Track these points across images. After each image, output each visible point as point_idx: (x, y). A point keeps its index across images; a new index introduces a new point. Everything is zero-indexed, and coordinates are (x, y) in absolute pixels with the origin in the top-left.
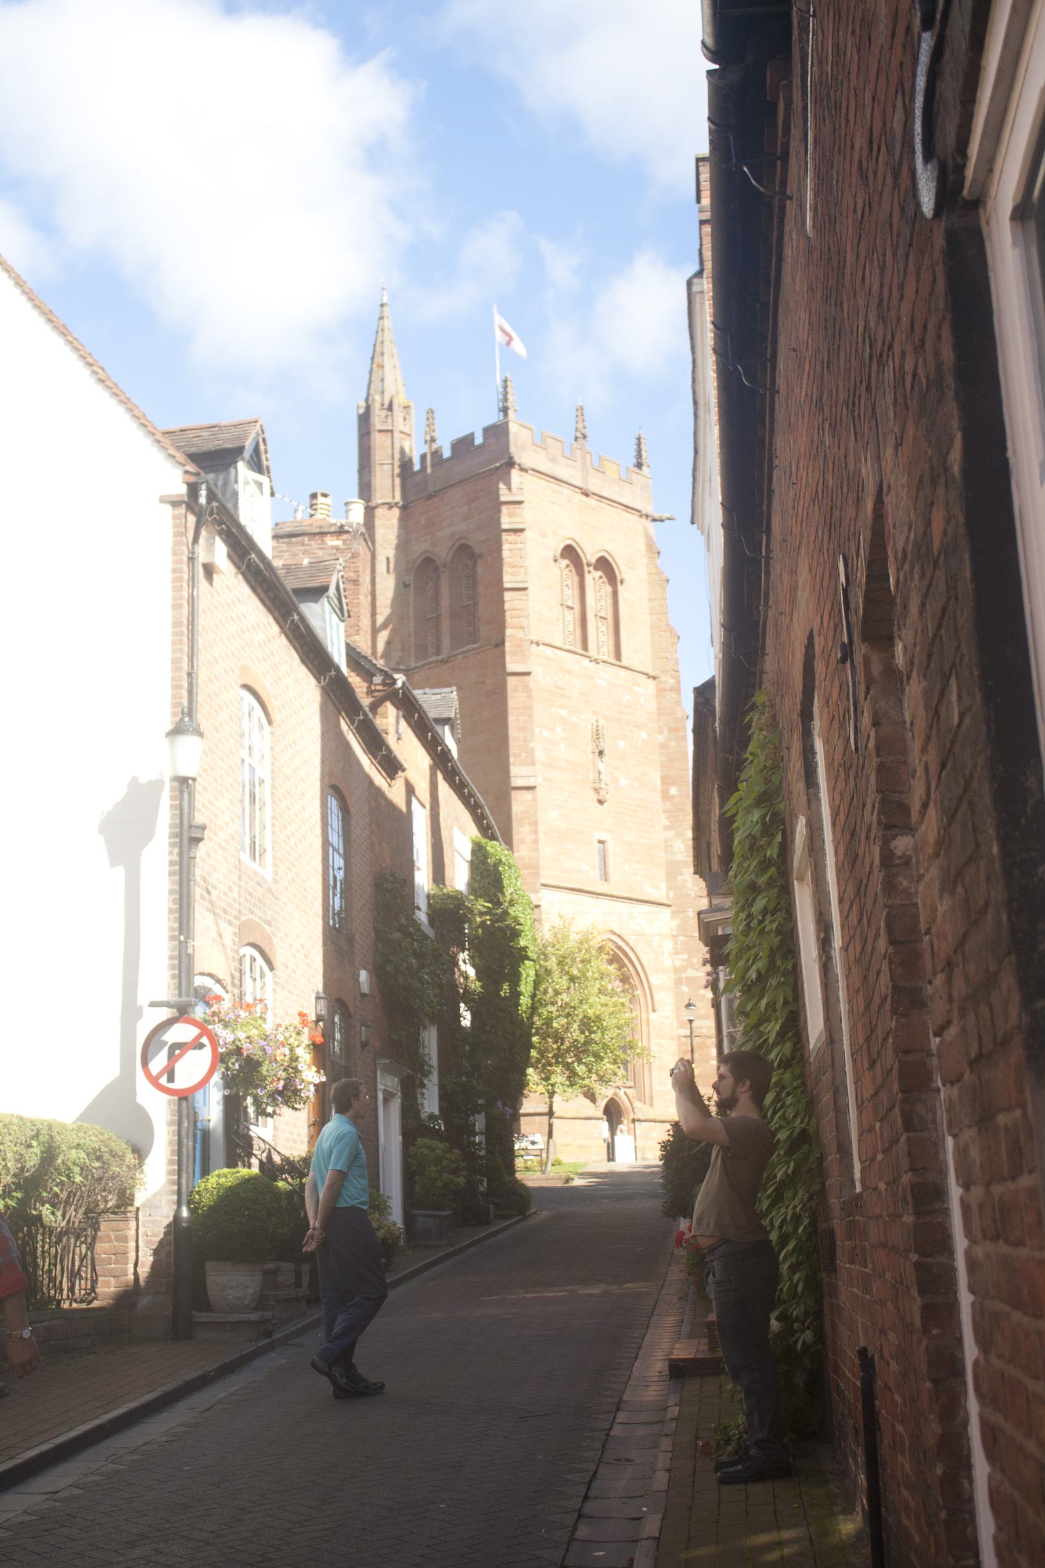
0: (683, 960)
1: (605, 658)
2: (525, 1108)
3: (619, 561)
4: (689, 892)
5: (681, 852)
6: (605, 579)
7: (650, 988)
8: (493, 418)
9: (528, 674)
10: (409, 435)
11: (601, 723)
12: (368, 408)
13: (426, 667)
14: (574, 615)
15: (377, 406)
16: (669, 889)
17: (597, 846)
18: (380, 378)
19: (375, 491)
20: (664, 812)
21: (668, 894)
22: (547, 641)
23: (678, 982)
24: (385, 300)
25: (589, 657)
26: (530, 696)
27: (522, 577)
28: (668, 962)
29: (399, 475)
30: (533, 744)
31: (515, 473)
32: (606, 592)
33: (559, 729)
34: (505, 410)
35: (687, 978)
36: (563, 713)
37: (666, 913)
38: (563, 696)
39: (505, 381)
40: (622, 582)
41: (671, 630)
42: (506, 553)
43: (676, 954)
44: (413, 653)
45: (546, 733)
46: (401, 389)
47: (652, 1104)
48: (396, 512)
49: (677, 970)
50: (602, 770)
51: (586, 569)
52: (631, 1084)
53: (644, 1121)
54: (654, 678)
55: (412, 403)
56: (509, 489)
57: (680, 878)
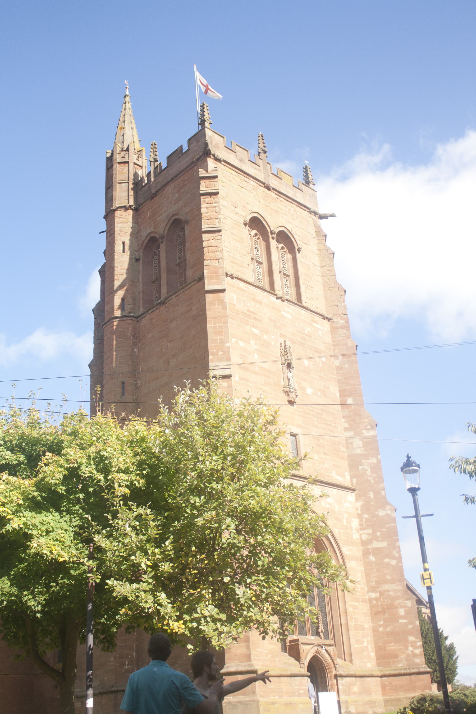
0: (368, 534)
1: (289, 298)
2: (228, 667)
3: (295, 236)
4: (369, 478)
5: (360, 447)
6: (286, 249)
7: (342, 557)
8: (195, 129)
9: (223, 291)
10: (142, 167)
11: (288, 343)
12: (112, 154)
13: (150, 312)
14: (263, 267)
15: (118, 149)
16: (352, 477)
17: (288, 436)
18: (122, 135)
19: (116, 199)
20: (343, 417)
21: (351, 481)
22: (240, 276)
23: (366, 553)
24: (127, 93)
25: (276, 295)
26: (225, 308)
27: (217, 225)
28: (356, 536)
29: (132, 189)
30: (228, 345)
31: (211, 163)
32: (287, 258)
33: (252, 342)
34: (202, 123)
35: (373, 549)
36: (256, 331)
37: (351, 497)
38: (255, 319)
39: (202, 107)
40: (299, 251)
41: (339, 287)
42: (203, 210)
43: (362, 529)
44: (141, 305)
45: (241, 344)
46: (136, 139)
47: (351, 661)
48: (131, 212)
49: (364, 543)
50: (291, 378)
51: (270, 236)
52: (332, 642)
53: (346, 677)
54: (329, 320)
55: (143, 149)
56: (207, 171)
57: (360, 468)
